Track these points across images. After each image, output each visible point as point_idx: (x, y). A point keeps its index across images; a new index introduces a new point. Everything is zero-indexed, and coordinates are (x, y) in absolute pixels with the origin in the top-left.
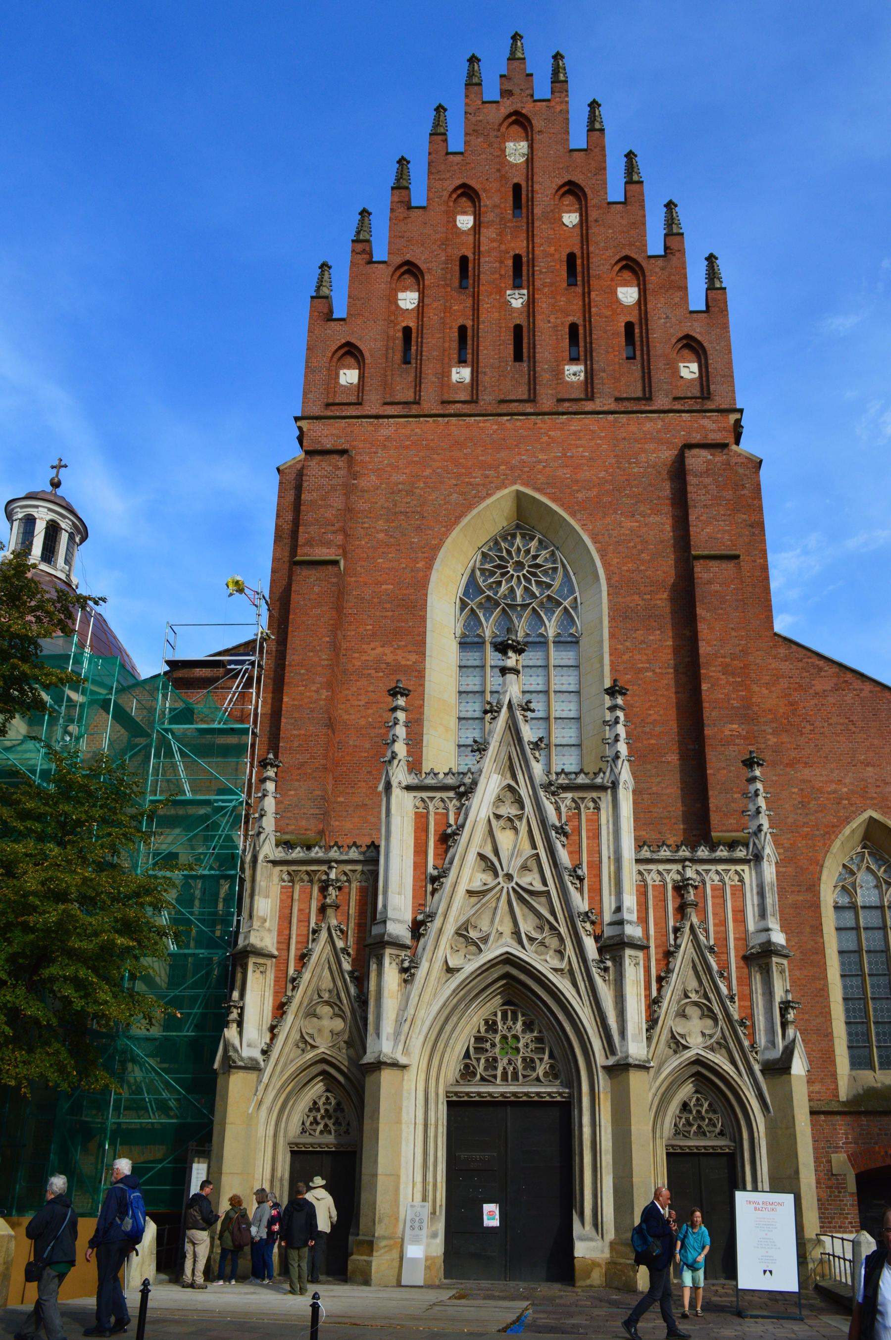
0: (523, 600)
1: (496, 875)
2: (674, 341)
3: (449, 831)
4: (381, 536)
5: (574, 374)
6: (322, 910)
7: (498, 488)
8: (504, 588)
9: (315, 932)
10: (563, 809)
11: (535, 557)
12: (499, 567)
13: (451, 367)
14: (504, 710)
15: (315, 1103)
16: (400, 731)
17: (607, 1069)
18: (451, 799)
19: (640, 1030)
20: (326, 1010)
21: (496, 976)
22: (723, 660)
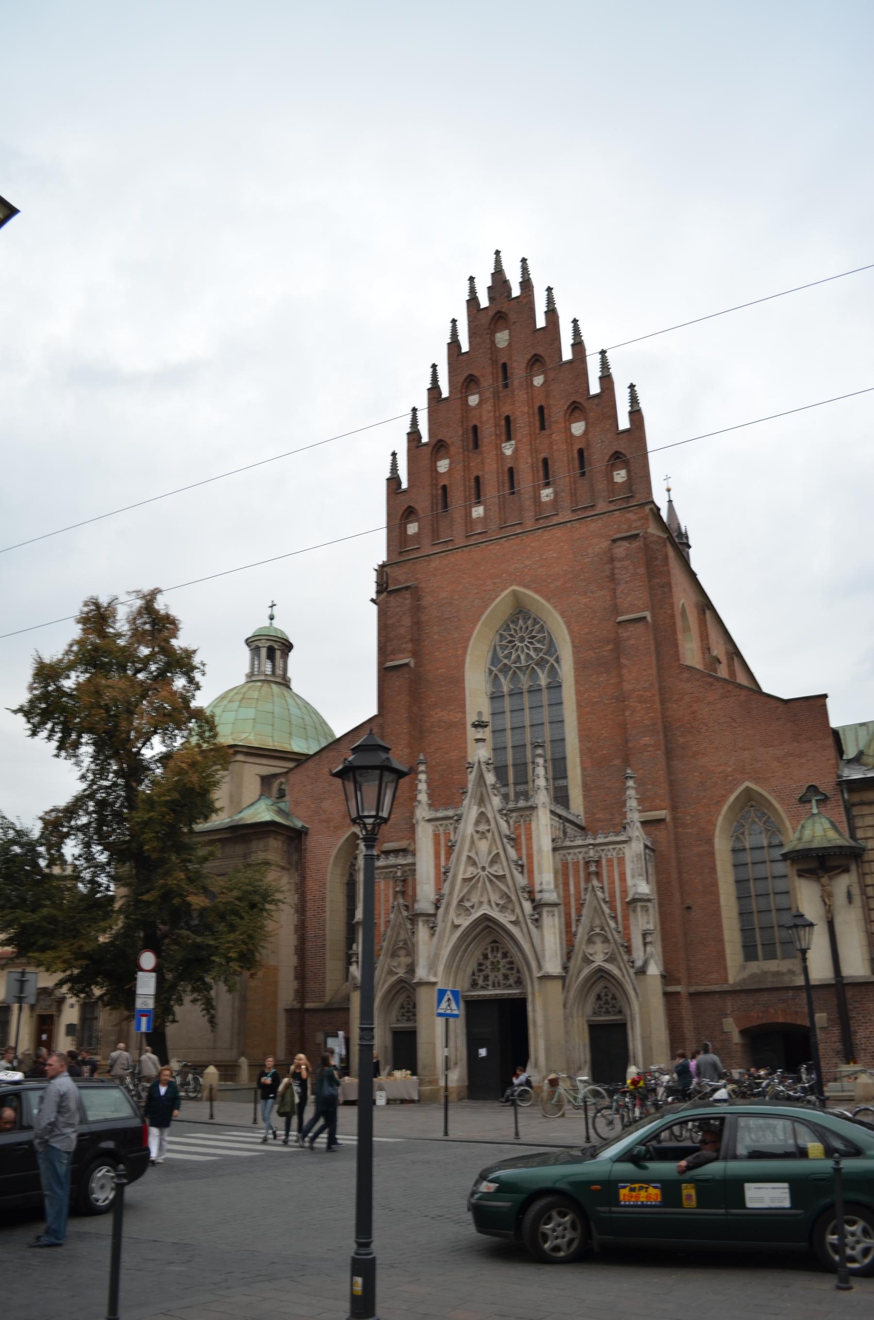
0: (527, 661)
2: (607, 458)
3: (450, 844)
4: (436, 637)
5: (547, 496)
6: (396, 893)
7: (503, 590)
8: (513, 657)
9: (393, 907)
10: (512, 823)
11: (532, 631)
12: (510, 642)
13: (471, 508)
14: (476, 766)
15: (402, 1004)
16: (422, 786)
17: (540, 978)
18: (451, 824)
19: (556, 954)
20: (402, 952)
21: (480, 927)
22: (637, 693)
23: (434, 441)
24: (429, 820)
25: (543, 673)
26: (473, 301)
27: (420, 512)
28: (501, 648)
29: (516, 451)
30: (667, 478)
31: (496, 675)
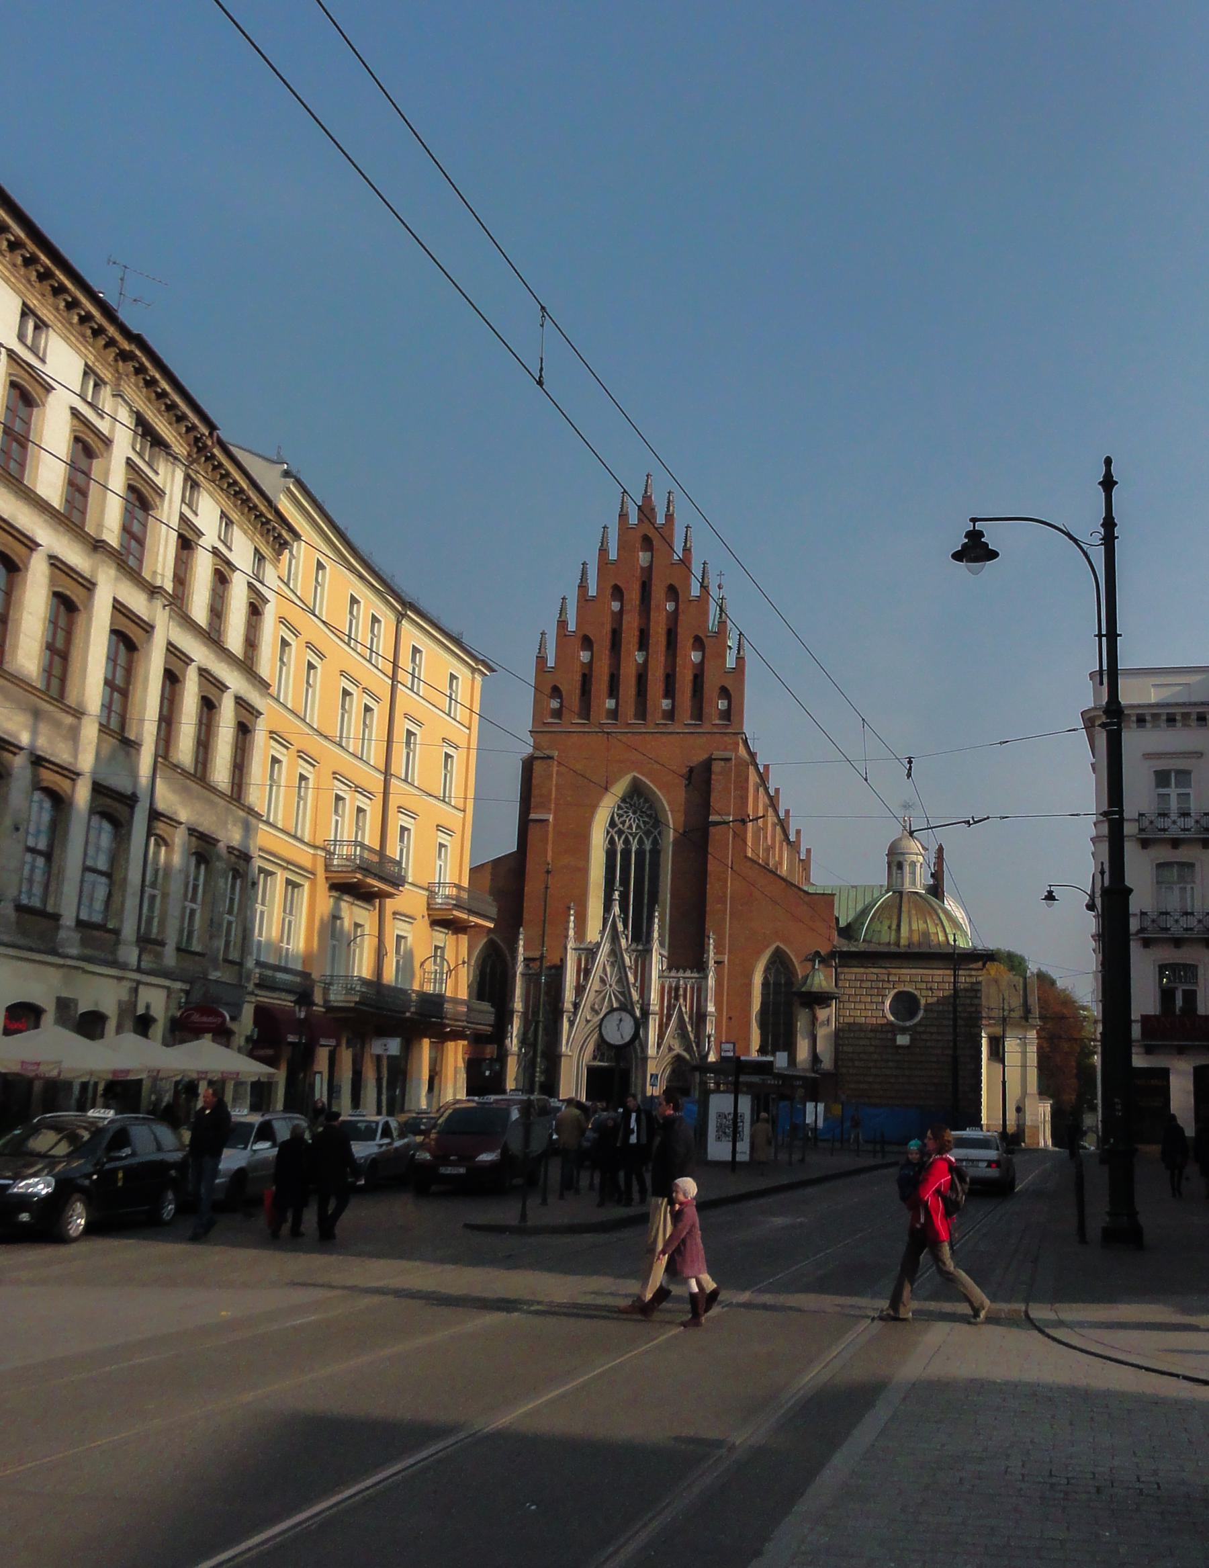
1: (606, 985)
8: (627, 824)
16: (572, 925)
23: (580, 634)
24: (575, 949)
25: (648, 840)
26: (623, 516)
27: (564, 693)
28: (617, 815)
29: (646, 661)
30: (721, 574)
31: (612, 836)
